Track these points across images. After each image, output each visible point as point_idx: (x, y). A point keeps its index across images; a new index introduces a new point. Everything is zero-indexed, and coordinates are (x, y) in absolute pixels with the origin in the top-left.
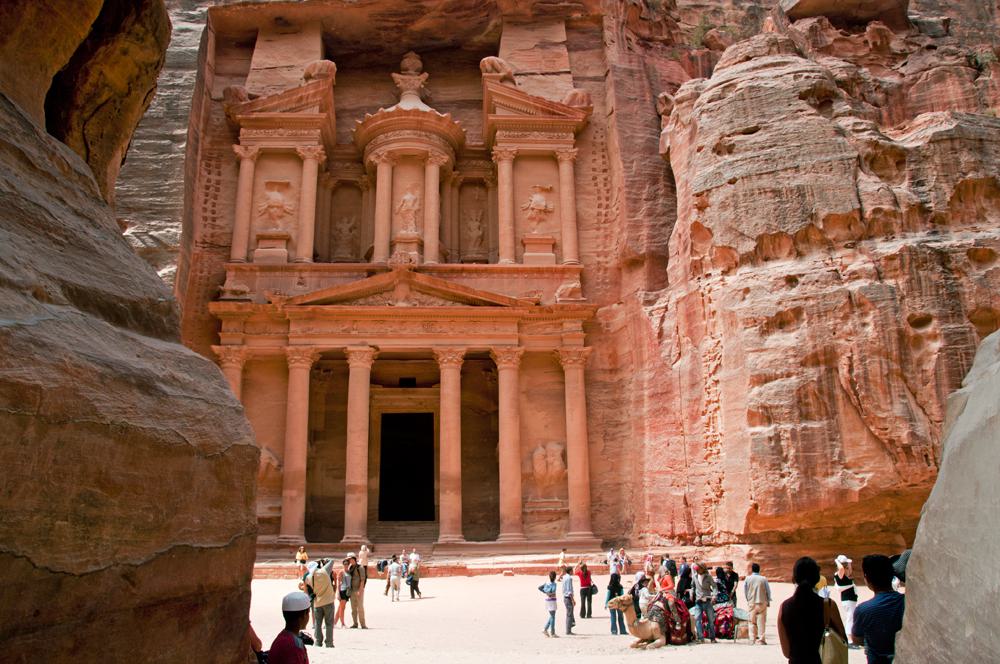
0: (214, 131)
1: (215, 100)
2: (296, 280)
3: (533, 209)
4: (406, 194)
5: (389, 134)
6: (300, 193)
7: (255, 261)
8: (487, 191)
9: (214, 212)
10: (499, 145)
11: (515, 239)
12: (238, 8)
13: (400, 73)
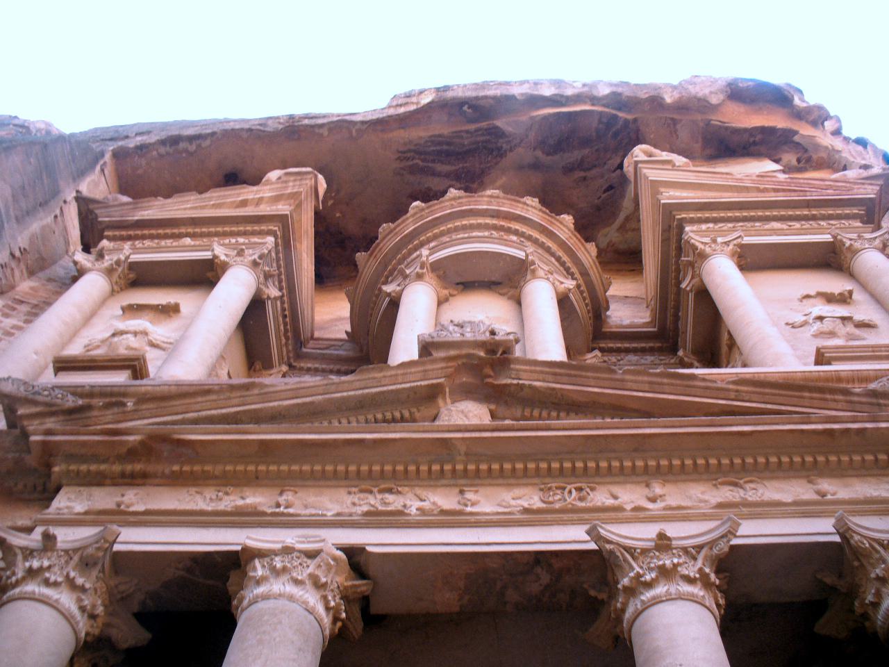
3: (821, 318)
12: (162, 150)
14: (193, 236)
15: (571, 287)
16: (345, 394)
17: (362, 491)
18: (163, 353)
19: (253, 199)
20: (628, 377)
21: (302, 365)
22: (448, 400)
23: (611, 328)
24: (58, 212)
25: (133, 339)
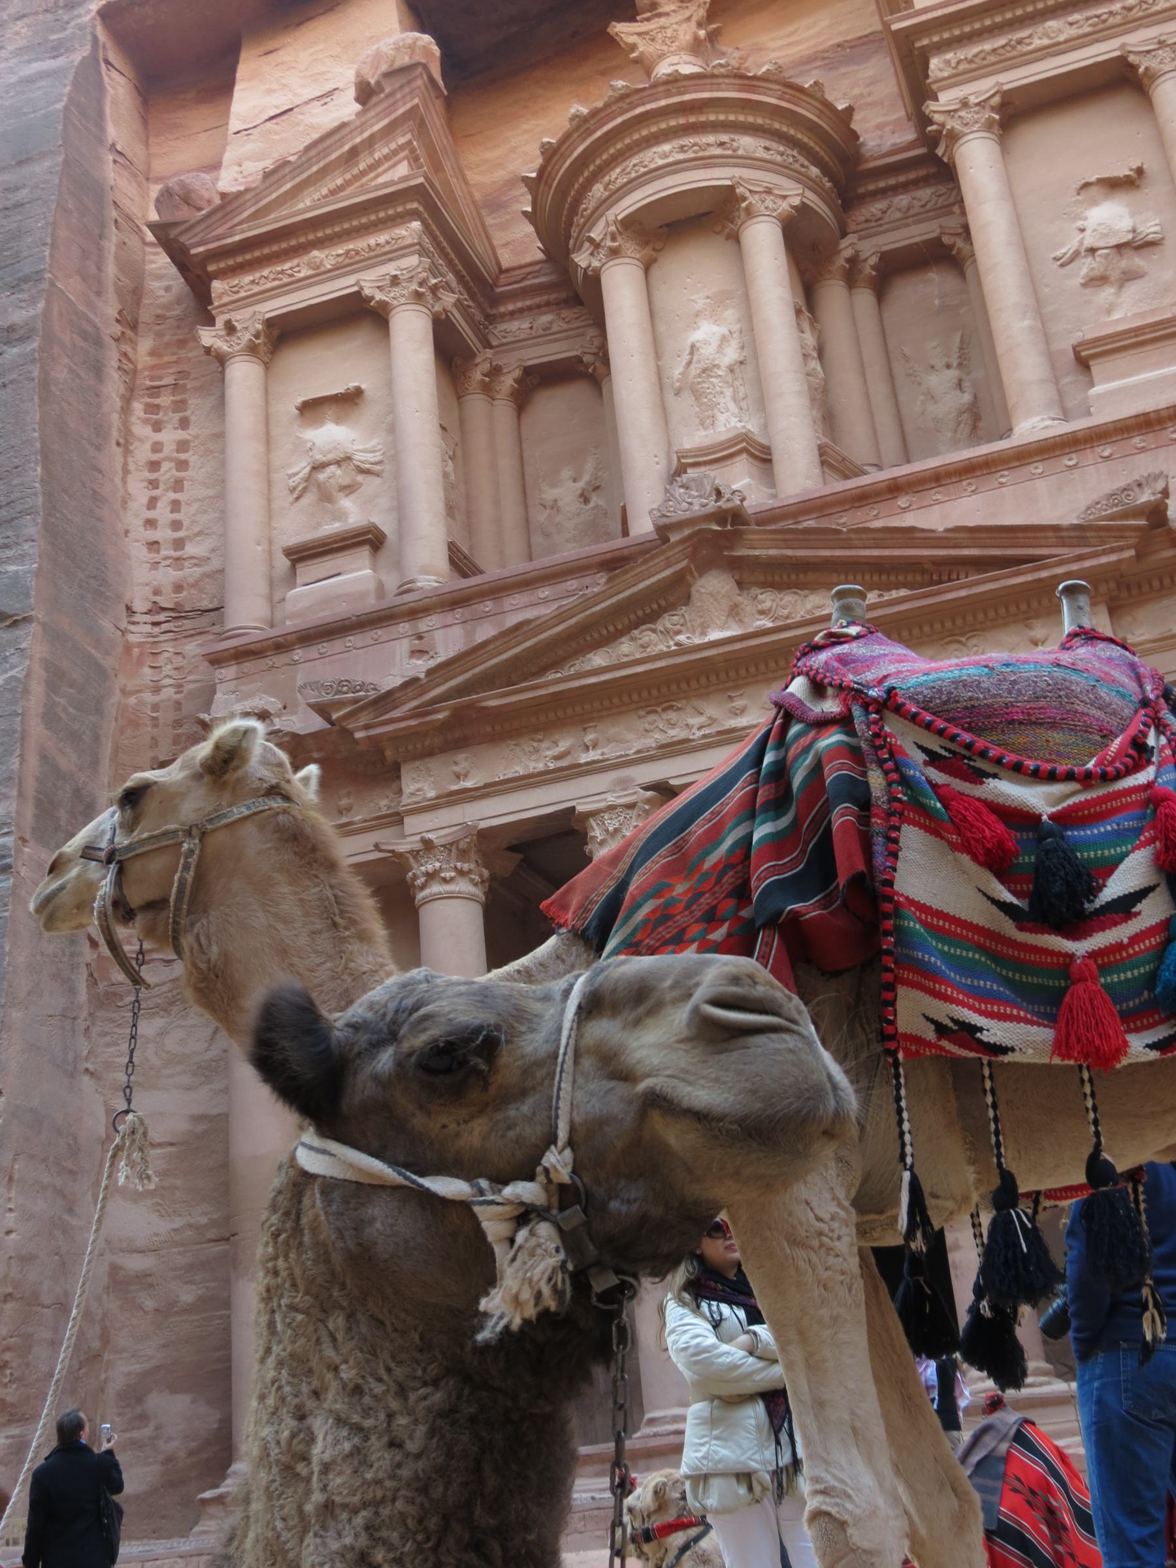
0: (158, 316)
1: (151, 244)
2: (404, 646)
3: (1092, 251)
4: (693, 325)
5: (614, 174)
6: (391, 409)
7: (288, 623)
8: (962, 275)
9: (176, 525)
10: (944, 97)
11: (1051, 357)
13: (632, 19)
14: (319, 244)
15: (796, 201)
16: (603, 605)
17: (649, 713)
18: (378, 480)
19: (362, 142)
20: (853, 536)
21: (502, 309)
22: (696, 574)
23: (867, 161)
24: (114, 214)
25: (339, 472)
